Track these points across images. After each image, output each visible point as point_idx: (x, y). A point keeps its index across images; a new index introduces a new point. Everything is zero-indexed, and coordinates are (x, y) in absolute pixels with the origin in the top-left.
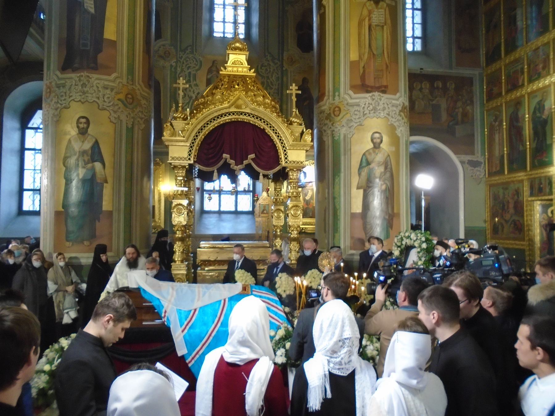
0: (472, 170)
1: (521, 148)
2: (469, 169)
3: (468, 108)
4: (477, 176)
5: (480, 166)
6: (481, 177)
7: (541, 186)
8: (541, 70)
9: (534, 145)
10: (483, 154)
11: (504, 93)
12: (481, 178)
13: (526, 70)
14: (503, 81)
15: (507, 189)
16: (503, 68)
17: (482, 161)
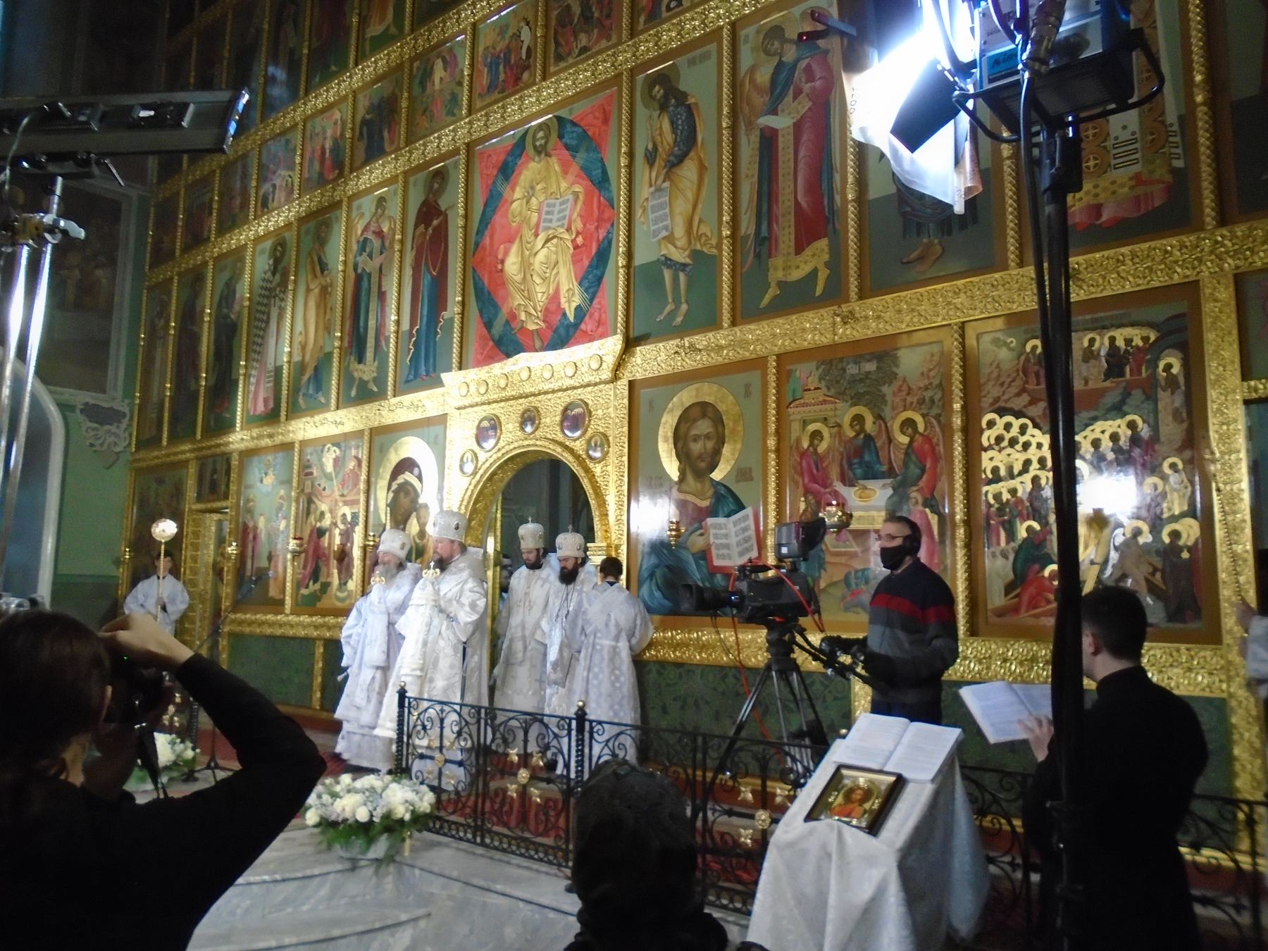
0: (94, 429)
1: (193, 387)
2: (84, 429)
3: (99, 272)
4: (106, 446)
5: (119, 422)
6: (118, 449)
7: (215, 477)
8: (237, 210)
9: (212, 382)
10: (128, 394)
11: (178, 253)
12: (118, 454)
13: (215, 206)
14: (180, 223)
15: (160, 481)
16: (182, 192)
17: (127, 410)
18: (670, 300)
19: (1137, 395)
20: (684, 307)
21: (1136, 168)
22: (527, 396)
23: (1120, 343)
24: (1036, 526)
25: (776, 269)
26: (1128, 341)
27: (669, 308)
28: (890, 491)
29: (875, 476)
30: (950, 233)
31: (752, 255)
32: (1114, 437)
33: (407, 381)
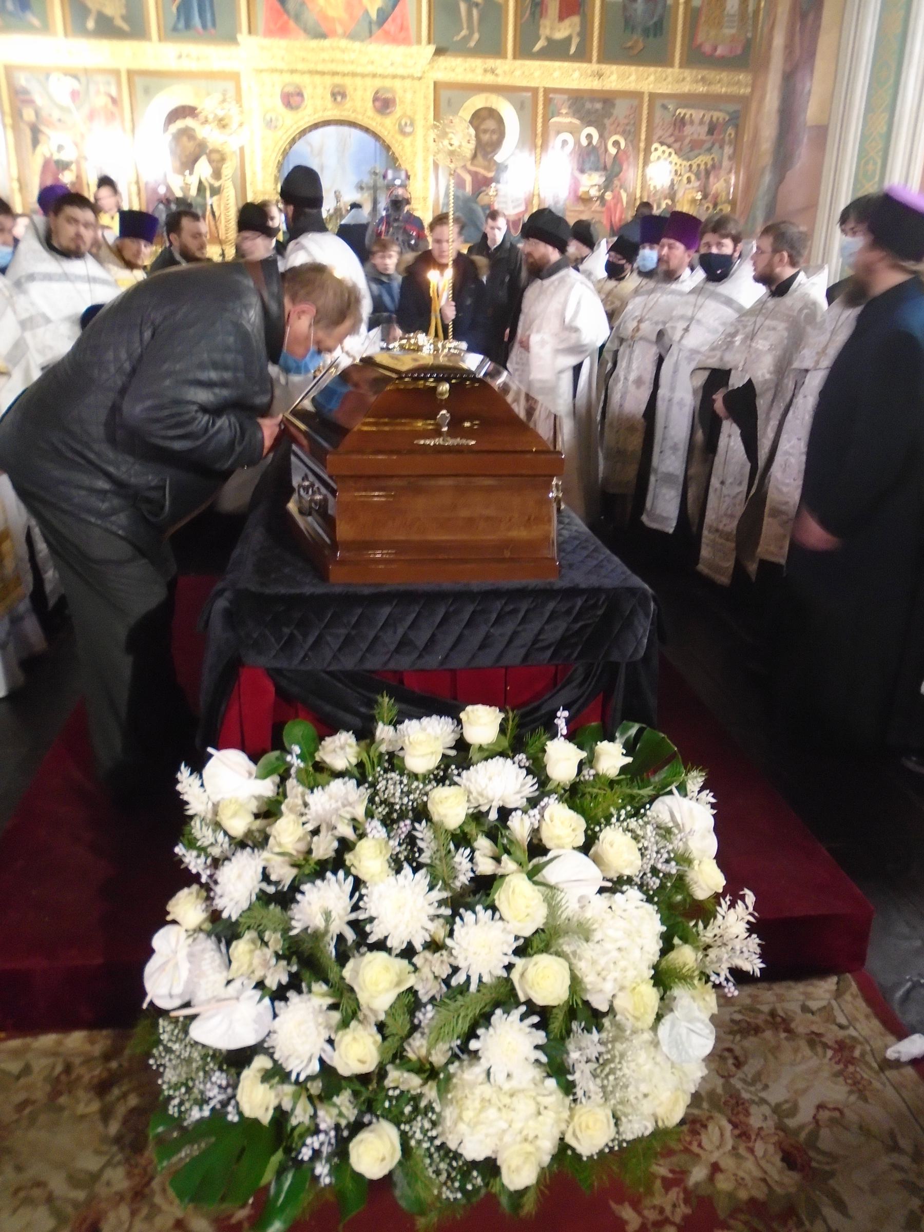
18: (465, 26)
19: (717, 146)
20: (476, 36)
21: (733, 31)
22: (334, 74)
23: (714, 119)
24: (670, 202)
25: (545, 27)
26: (718, 119)
27: (464, 32)
28: (604, 179)
29: (597, 170)
30: (648, 36)
31: (528, 12)
32: (706, 164)
33: (175, 29)
